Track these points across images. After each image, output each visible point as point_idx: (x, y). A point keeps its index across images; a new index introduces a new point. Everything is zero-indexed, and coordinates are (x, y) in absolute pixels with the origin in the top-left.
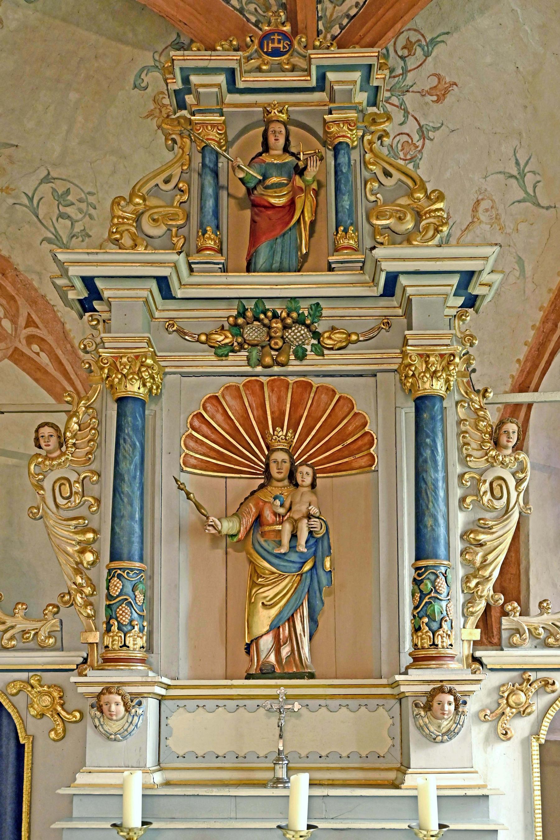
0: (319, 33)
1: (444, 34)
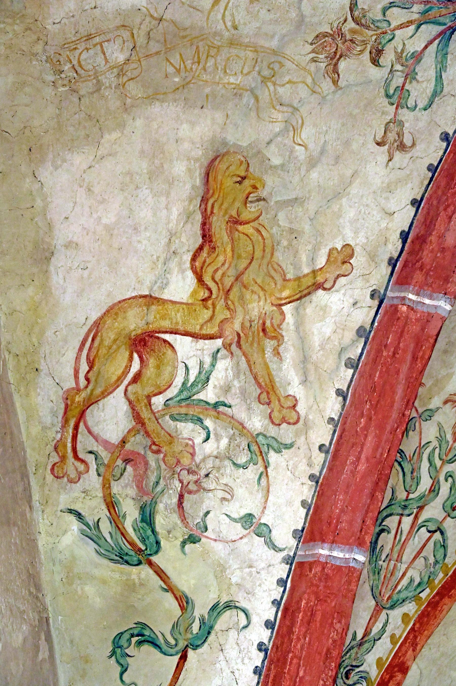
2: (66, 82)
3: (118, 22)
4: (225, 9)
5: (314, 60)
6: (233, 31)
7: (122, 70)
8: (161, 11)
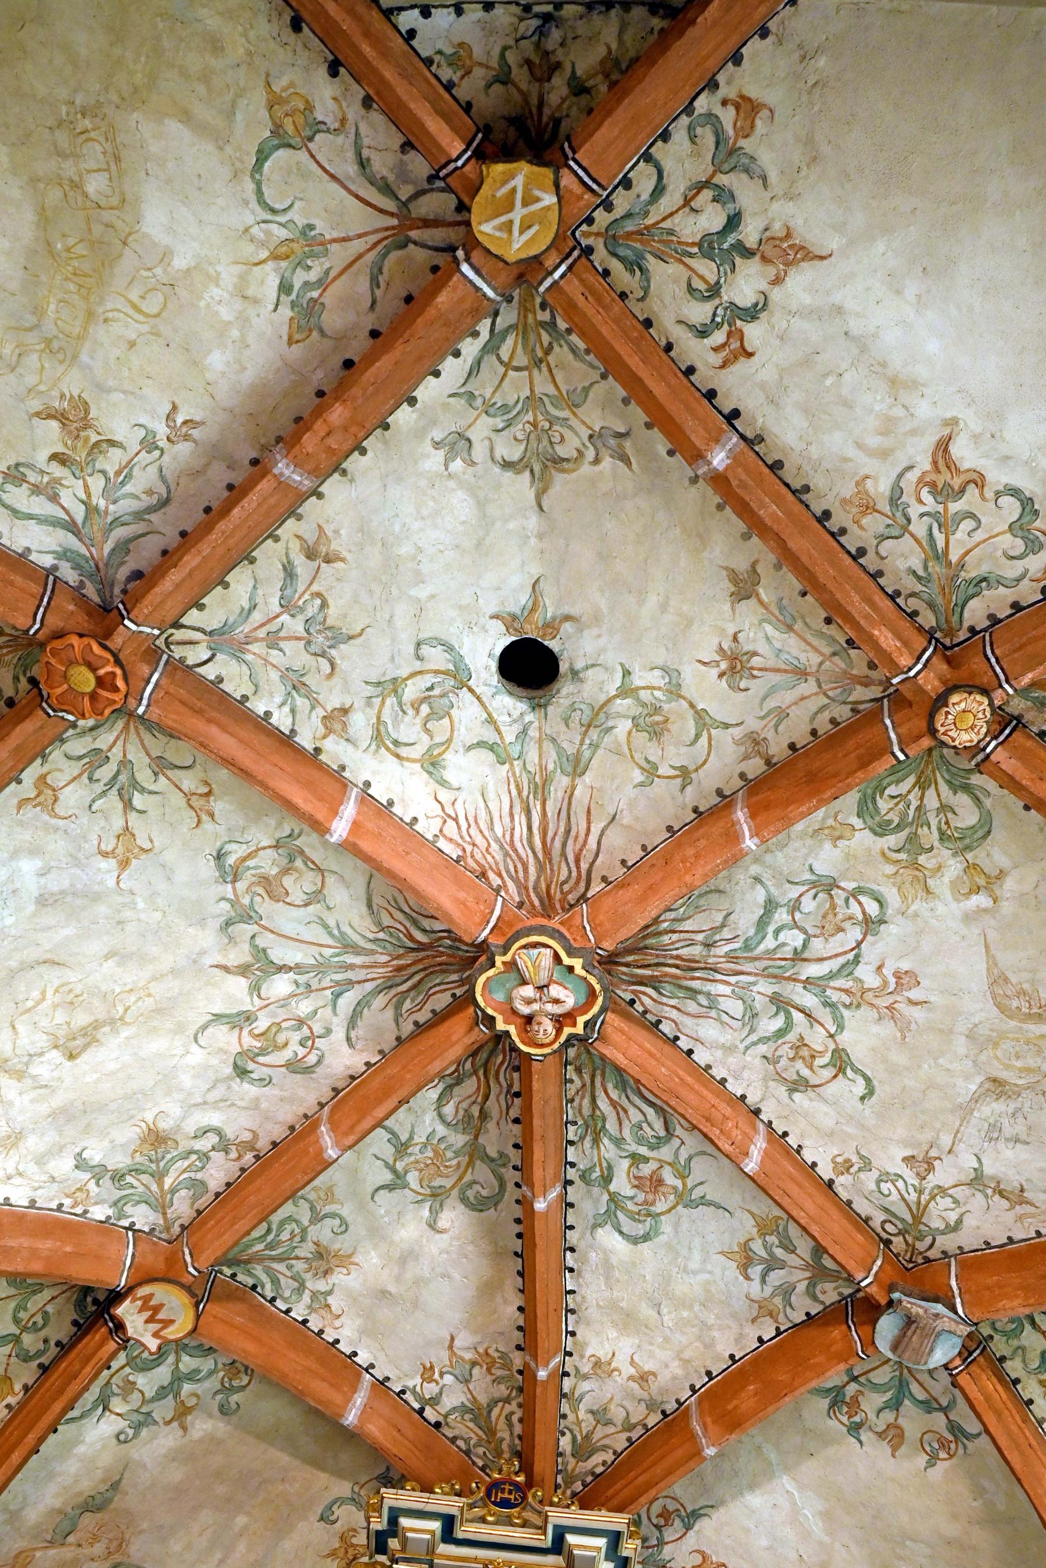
0: (557, 1487)
2: (71, 117)
3: (129, 196)
4: (126, 314)
5: (62, 396)
6: (101, 318)
7: (77, 186)
8: (133, 245)
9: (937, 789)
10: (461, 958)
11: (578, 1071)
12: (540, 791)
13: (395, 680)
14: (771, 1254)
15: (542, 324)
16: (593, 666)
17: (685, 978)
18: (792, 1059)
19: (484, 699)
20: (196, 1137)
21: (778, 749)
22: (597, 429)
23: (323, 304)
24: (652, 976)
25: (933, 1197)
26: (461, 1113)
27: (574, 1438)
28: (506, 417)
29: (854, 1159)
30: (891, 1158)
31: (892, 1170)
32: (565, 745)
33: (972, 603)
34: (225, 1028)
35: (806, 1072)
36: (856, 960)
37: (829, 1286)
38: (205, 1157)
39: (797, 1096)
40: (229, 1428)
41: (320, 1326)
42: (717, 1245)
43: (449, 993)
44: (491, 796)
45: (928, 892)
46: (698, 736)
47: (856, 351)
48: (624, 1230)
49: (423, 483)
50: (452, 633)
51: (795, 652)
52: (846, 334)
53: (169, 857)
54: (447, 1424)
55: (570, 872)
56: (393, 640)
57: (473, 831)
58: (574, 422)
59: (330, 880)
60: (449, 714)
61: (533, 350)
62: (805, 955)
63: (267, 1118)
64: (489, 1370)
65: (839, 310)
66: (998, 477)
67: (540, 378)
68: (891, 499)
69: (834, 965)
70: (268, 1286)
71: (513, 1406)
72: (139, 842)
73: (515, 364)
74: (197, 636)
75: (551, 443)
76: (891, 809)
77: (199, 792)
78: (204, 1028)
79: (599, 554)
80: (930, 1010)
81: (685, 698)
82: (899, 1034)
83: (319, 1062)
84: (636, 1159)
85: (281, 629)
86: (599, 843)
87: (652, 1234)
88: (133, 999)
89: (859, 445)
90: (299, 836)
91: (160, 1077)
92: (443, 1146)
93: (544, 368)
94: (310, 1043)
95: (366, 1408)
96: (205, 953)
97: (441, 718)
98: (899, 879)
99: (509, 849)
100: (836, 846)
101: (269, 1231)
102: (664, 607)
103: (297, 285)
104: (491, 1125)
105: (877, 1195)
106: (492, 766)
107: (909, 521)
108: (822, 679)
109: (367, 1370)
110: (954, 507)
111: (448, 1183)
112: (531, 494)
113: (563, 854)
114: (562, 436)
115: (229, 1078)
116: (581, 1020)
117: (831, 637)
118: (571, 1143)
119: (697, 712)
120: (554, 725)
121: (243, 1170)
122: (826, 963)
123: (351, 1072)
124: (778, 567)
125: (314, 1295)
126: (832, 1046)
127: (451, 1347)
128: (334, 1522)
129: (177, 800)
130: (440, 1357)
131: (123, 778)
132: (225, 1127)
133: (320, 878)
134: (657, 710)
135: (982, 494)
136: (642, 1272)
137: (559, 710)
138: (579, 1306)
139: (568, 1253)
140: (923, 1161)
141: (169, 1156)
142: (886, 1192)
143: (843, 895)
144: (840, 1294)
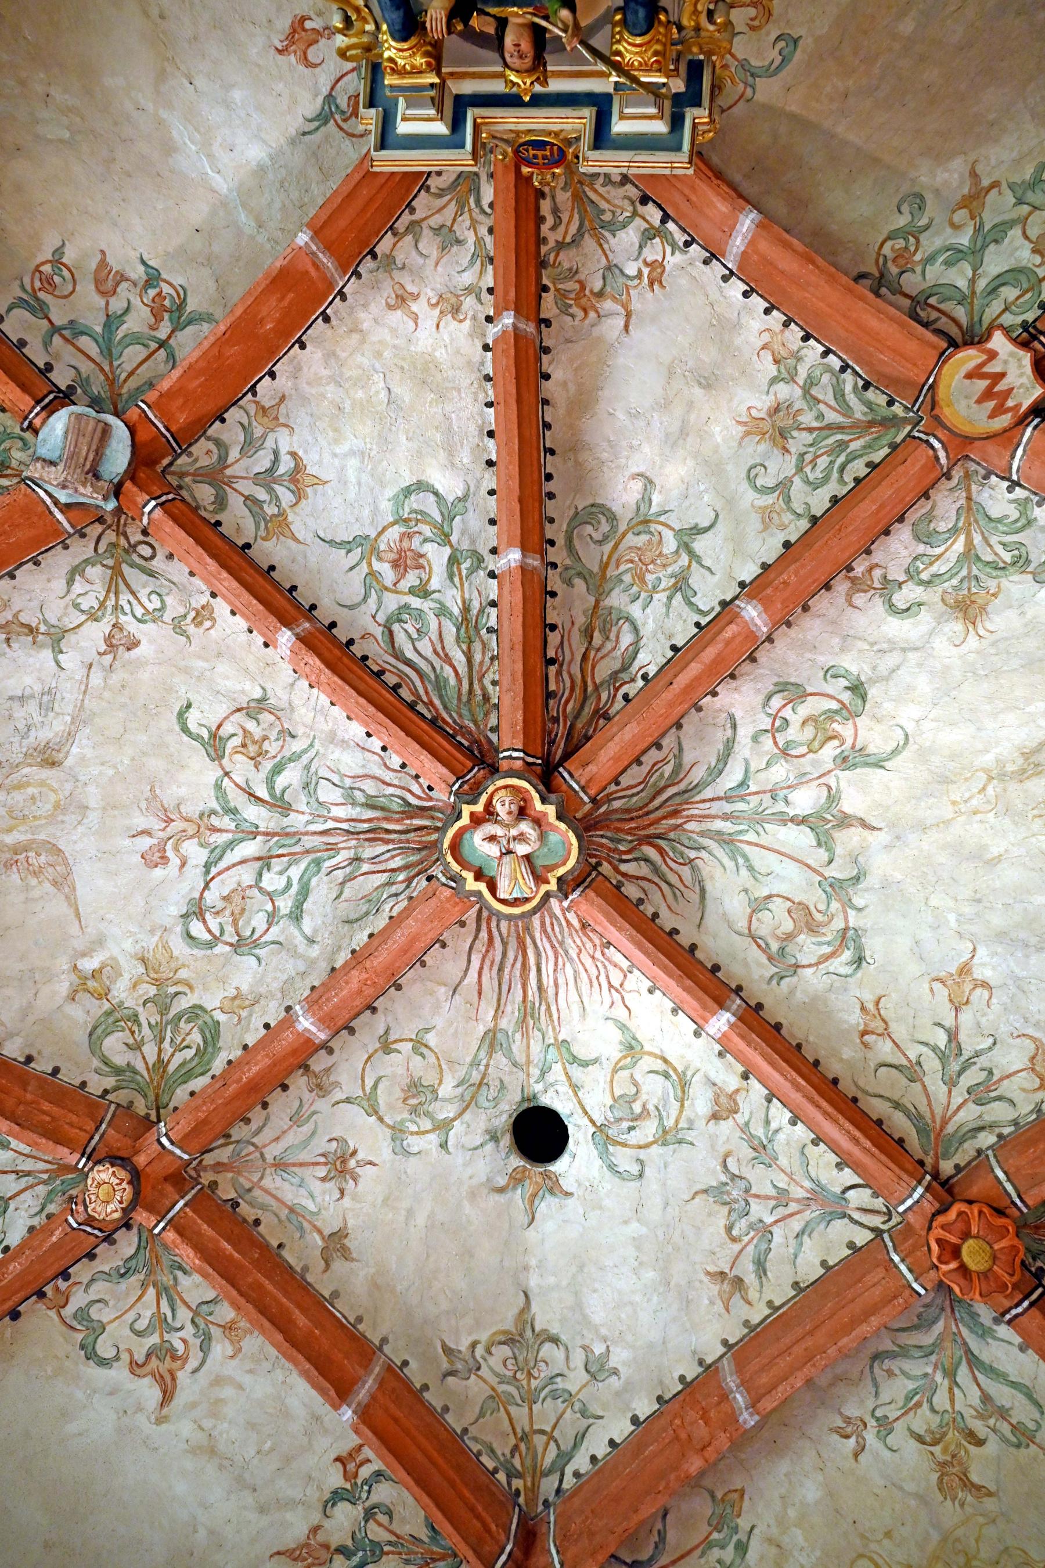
1: (309, 133)
9: (146, 1063)
10: (608, 827)
11: (486, 698)
12: (529, 1010)
13: (664, 1144)
14: (270, 491)
15: (520, 1475)
16: (475, 1149)
17: (378, 819)
18: (265, 738)
19: (580, 1111)
20: (920, 605)
21: (299, 1083)
22: (473, 1377)
23: (710, 1525)
24: (411, 818)
25: (102, 604)
26: (613, 636)
27: (478, 202)
28: (555, 1387)
29: (191, 629)
30: (153, 641)
31: (150, 626)
32: (504, 1060)
33: (131, 1251)
34: (871, 749)
35: (251, 726)
36: (207, 867)
37: (204, 462)
38: (911, 574)
39: (257, 694)
40: (913, 174)
41: (787, 332)
42: (330, 493)
43: (623, 785)
44: (576, 1008)
45: (143, 960)
46: (375, 1086)
47: (247, 1476)
48: (432, 498)
49: (629, 1338)
50: (608, 1183)
51: (287, 1186)
52: (255, 1490)
53: (914, 968)
54: (633, 203)
55: (498, 926)
56: (664, 1184)
57: (593, 972)
58: (493, 1380)
59: (742, 924)
60: (615, 1101)
61: (528, 1449)
62: (259, 864)
63: (833, 622)
64: (583, 287)
65: (262, 1510)
66: (119, 1373)
67: (523, 1423)
68: (210, 1339)
69: (231, 858)
70: (848, 388)
71: (553, 238)
72: (946, 992)
73: (545, 1438)
74: (856, 1216)
75: (515, 1358)
76: (188, 1034)
77: (874, 1037)
78: (896, 752)
79: (472, 1256)
80: (129, 828)
81: (388, 1126)
82: (158, 791)
83: (769, 698)
84: (422, 591)
85: (774, 1208)
86: (469, 961)
87: (402, 497)
88: (974, 802)
89: (240, 1387)
90: (772, 977)
91: (954, 693)
92: (635, 589)
93: (519, 1431)
94: (778, 723)
95: (729, 231)
96: (886, 847)
97: (622, 1096)
98: (173, 965)
99: (558, 949)
100: (237, 989)
101: (842, 469)
102: (410, 1213)
103: (731, 1547)
104: (581, 620)
105: (163, 591)
106: (574, 1039)
107: (193, 1321)
108: (261, 1162)
109: (732, 273)
110: (154, 1339)
111: (631, 540)
112: (535, 1308)
113: (505, 944)
114: (505, 1365)
115: (873, 681)
116: (465, 820)
117: (253, 1207)
118: (493, 604)
119: (376, 1112)
120: (515, 1082)
121: (868, 552)
122: (238, 859)
123: (734, 684)
124: (306, 1269)
125: (792, 379)
126: (225, 761)
127: (628, 315)
128: (778, 38)
129: (899, 1031)
130: (642, 300)
131: (955, 1067)
132: (884, 615)
133: (753, 927)
134: (414, 1110)
135: (131, 1355)
136: (410, 444)
137: (509, 1097)
138: (480, 386)
139: (494, 459)
140: (117, 646)
141: (955, 582)
142: (154, 597)
143: (227, 938)
144: (190, 455)
